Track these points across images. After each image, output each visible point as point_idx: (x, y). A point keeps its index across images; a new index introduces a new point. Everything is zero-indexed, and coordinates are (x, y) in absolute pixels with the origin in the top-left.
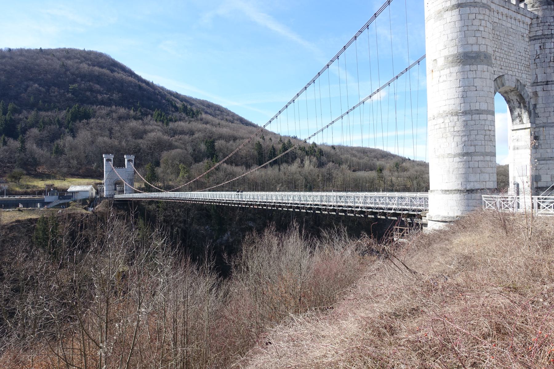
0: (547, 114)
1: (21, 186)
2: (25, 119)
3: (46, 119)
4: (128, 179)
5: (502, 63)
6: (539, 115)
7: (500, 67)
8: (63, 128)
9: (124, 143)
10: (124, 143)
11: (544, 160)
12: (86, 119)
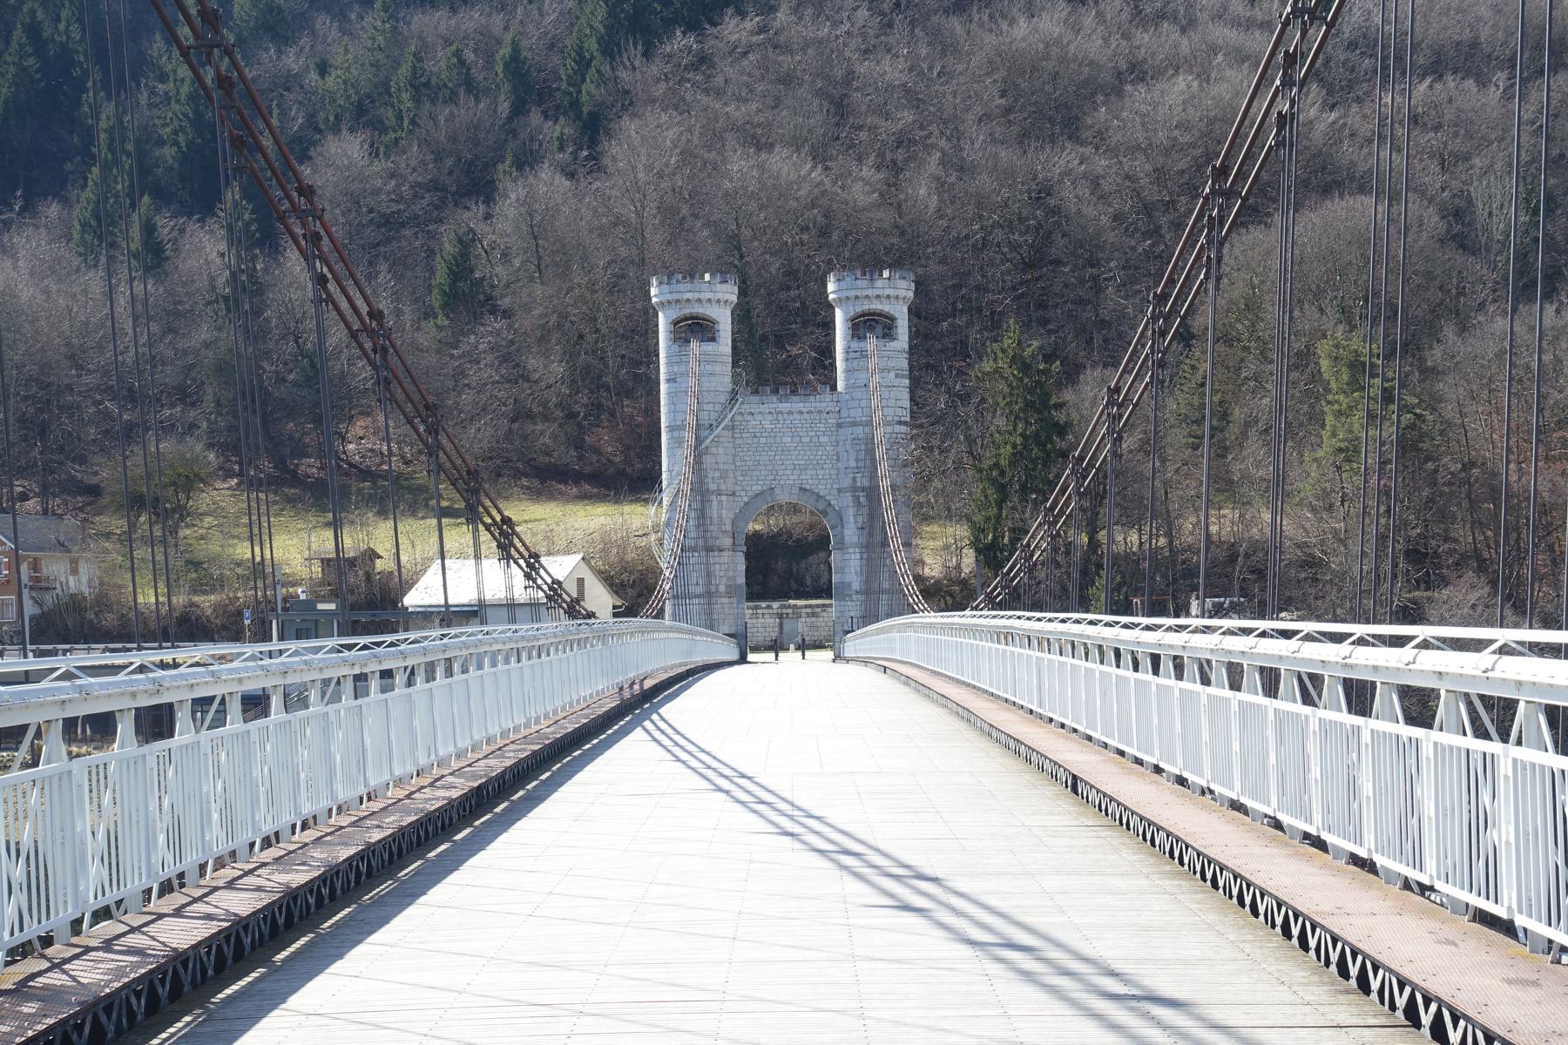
1: (166, 576)
2: (314, 75)
3: (439, 64)
4: (854, 489)
8: (535, 117)
9: (922, 191)
10: (922, 191)
12: (692, 27)
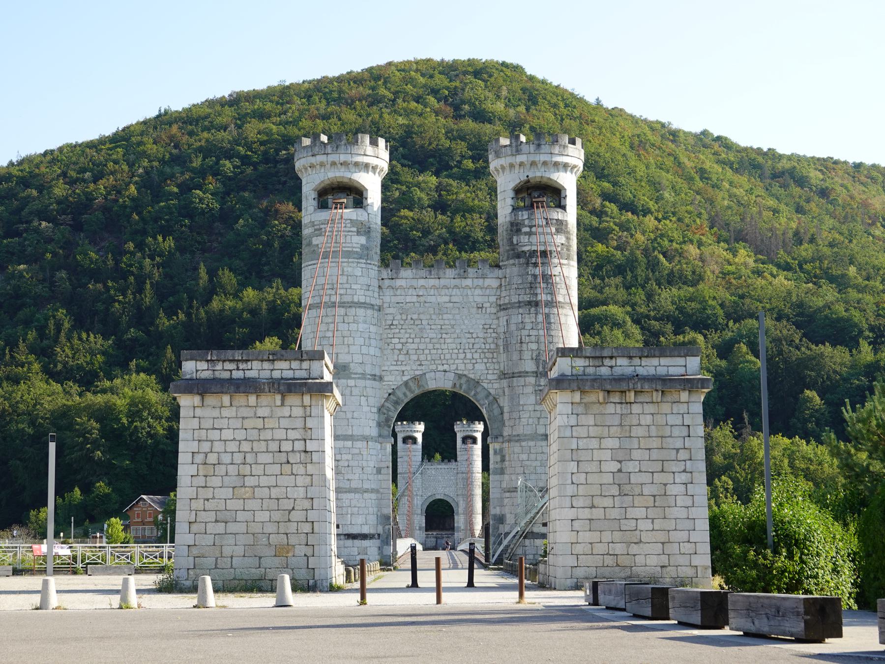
0: (511, 423)
5: (422, 357)
6: (507, 424)
7: (419, 363)
11: (509, 492)
